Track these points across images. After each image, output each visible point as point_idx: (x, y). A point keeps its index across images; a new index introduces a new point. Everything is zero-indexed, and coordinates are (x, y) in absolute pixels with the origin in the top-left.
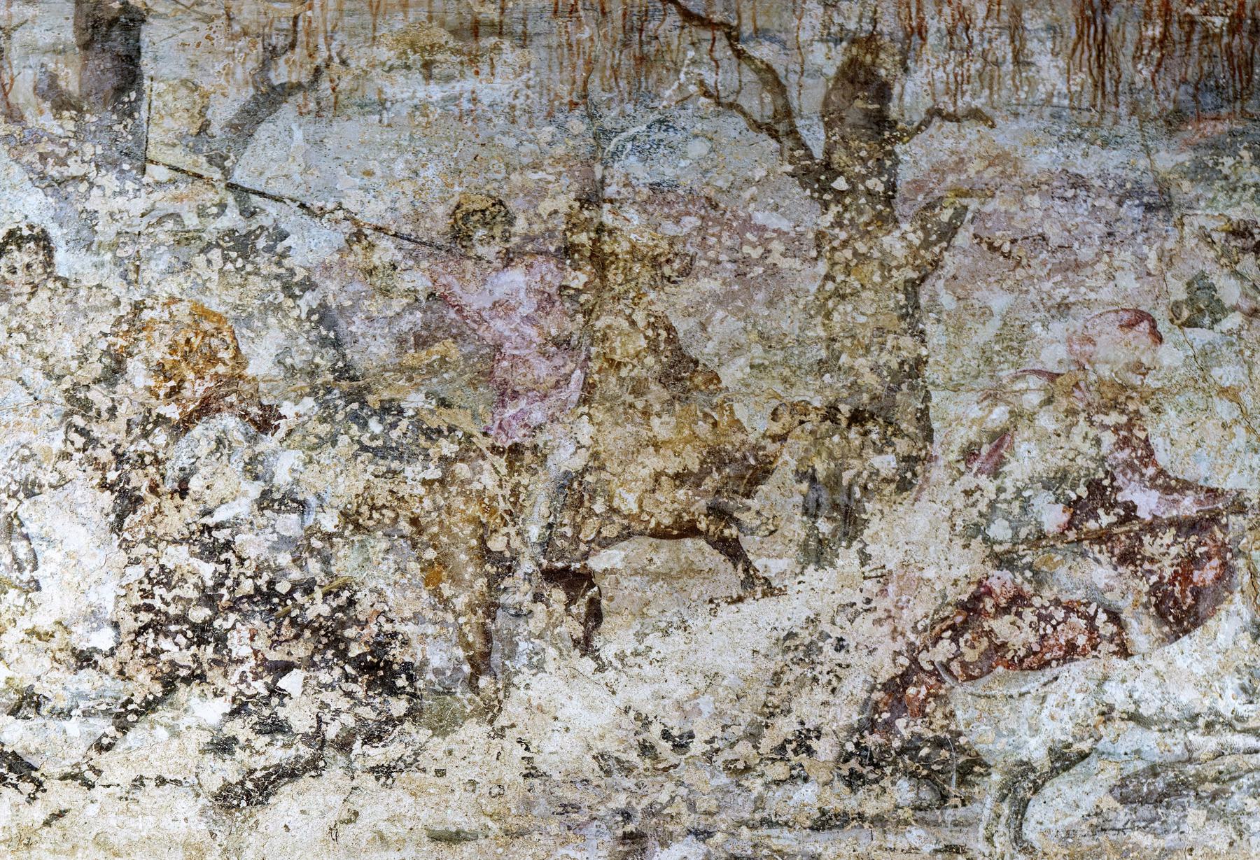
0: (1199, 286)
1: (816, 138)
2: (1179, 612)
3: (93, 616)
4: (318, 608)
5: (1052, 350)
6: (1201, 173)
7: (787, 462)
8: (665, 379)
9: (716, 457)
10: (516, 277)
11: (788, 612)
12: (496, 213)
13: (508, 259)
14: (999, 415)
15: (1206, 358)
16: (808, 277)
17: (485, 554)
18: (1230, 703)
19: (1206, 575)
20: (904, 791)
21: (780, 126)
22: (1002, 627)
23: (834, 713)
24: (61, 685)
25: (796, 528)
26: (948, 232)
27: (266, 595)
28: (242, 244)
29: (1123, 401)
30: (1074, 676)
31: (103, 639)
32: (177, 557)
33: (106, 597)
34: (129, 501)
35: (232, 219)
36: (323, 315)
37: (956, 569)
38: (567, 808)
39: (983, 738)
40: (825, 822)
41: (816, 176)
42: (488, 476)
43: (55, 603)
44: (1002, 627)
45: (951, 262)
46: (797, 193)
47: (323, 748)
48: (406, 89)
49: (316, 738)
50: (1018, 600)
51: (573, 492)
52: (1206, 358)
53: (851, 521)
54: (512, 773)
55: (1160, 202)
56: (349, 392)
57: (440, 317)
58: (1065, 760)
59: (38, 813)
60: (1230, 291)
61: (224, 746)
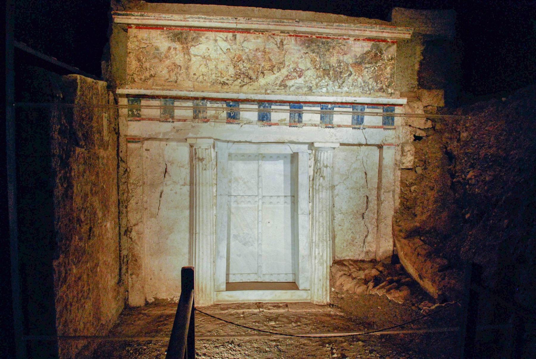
1: (279, 45)
2: (300, 77)
5: (293, 59)
10: (259, 53)
12: (259, 49)
16: (278, 54)
18: (303, 82)
20: (283, 87)
21: (276, 44)
23: (278, 82)
24: (230, 78)
28: (242, 50)
29: (297, 63)
30: (293, 81)
32: (238, 70)
33: (233, 73)
37: (286, 73)
39: (288, 84)
41: (279, 48)
42: (258, 66)
43: (230, 73)
47: (247, 83)
48: (253, 40)
51: (263, 67)
53: (280, 70)
55: (299, 51)
56: (249, 60)
57: (255, 56)
58: (293, 86)
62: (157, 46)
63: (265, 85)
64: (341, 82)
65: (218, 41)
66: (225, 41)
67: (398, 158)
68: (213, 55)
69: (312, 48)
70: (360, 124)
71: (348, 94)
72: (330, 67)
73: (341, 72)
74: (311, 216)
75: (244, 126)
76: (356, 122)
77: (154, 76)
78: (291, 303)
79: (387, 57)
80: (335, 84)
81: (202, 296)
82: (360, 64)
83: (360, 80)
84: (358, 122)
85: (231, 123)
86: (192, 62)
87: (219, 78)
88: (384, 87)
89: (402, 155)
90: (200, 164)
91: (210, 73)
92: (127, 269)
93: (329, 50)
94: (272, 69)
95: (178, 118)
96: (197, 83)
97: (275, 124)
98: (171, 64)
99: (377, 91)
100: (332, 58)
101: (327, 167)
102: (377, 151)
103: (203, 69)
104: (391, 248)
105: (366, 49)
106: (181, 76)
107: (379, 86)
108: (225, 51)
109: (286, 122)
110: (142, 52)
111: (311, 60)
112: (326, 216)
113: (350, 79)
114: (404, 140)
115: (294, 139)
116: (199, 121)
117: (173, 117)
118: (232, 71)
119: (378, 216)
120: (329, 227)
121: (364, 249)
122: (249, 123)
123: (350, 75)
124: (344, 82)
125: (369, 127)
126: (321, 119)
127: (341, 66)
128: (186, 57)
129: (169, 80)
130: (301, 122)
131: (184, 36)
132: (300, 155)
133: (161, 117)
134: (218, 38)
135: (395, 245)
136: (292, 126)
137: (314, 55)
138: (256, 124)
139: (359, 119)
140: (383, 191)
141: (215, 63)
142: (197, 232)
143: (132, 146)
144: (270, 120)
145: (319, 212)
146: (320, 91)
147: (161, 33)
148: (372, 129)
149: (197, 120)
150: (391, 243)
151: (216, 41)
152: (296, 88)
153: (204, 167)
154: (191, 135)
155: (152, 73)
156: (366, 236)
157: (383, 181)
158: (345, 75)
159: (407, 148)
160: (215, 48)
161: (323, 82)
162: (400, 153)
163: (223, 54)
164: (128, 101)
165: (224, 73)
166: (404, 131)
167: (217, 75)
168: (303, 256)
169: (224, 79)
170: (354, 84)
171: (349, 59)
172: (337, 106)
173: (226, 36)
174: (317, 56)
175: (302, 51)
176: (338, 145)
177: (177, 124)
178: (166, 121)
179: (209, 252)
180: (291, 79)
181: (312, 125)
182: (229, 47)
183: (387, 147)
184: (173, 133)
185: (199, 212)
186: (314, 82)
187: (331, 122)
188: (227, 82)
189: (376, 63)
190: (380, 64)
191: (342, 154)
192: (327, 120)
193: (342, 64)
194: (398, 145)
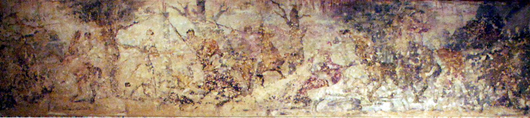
0: (336, 38)
1: (289, 18)
2: (335, 81)
3: (200, 81)
4: (229, 80)
6: (336, 24)
7: (287, 61)
8: (271, 50)
9: (278, 60)
10: (252, 37)
11: (287, 81)
12: (250, 28)
13: (252, 34)
14: (312, 55)
15: (337, 48)
17: (249, 73)
18: (341, 93)
19: (338, 76)
20: (302, 104)
21: (284, 17)
22: (313, 83)
23: (293, 94)
25: (288, 69)
26: (305, 31)
27: (222, 78)
28: (218, 32)
29: (327, 53)
31: (202, 84)
32: (211, 73)
33: (202, 79)
34: (205, 66)
35: (217, 28)
36: (229, 41)
37: (307, 75)
41: (289, 23)
42: (249, 62)
44: (313, 83)
45: (306, 35)
46: (288, 26)
48: (238, 11)
49: (229, 97)
50: (315, 79)
51: (260, 65)
52: (337, 48)
53: (294, 69)
54: (253, 102)
56: (232, 51)
58: (321, 100)
59: (194, 107)
60: (340, 39)
61: (217, 98)
62: (53, 32)
63: (265, 101)
64: (419, 89)
65: (170, 16)
66: (184, 15)
68: (162, 44)
69: (357, 20)
72: (395, 58)
73: (418, 69)
77: (51, 92)
79: (513, 31)
80: (407, 93)
82: (456, 49)
83: (458, 82)
86: (122, 60)
87: (175, 91)
88: (510, 95)
91: (157, 80)
93: (390, 23)
94: (277, 68)
96: (133, 103)
98: (81, 66)
100: (398, 41)
103: (144, 74)
105: (467, 18)
106: (101, 89)
107: (500, 93)
108: (184, 34)
110: (26, 44)
111: (357, 47)
113: (439, 82)
118: (199, 75)
123: (437, 73)
124: (425, 88)
127: (417, 55)
128: (110, 50)
129: (79, 98)
131: (105, 9)
134: (169, 10)
137: (361, 34)
141: (165, 59)
146: (377, 108)
147: (62, 6)
151: (166, 15)
155: (46, 85)
158: (427, 74)
160: (165, 30)
161: (384, 91)
163: (181, 41)
165: (185, 80)
167: (171, 85)
169: (185, 93)
170: (447, 92)
171: (432, 40)
173: (184, 5)
174: (367, 38)
175: (338, 29)
180: (317, 87)
182: (191, 27)
186: (364, 92)
188: (191, 97)
189: (490, 46)
190: (498, 49)
193: (419, 52)
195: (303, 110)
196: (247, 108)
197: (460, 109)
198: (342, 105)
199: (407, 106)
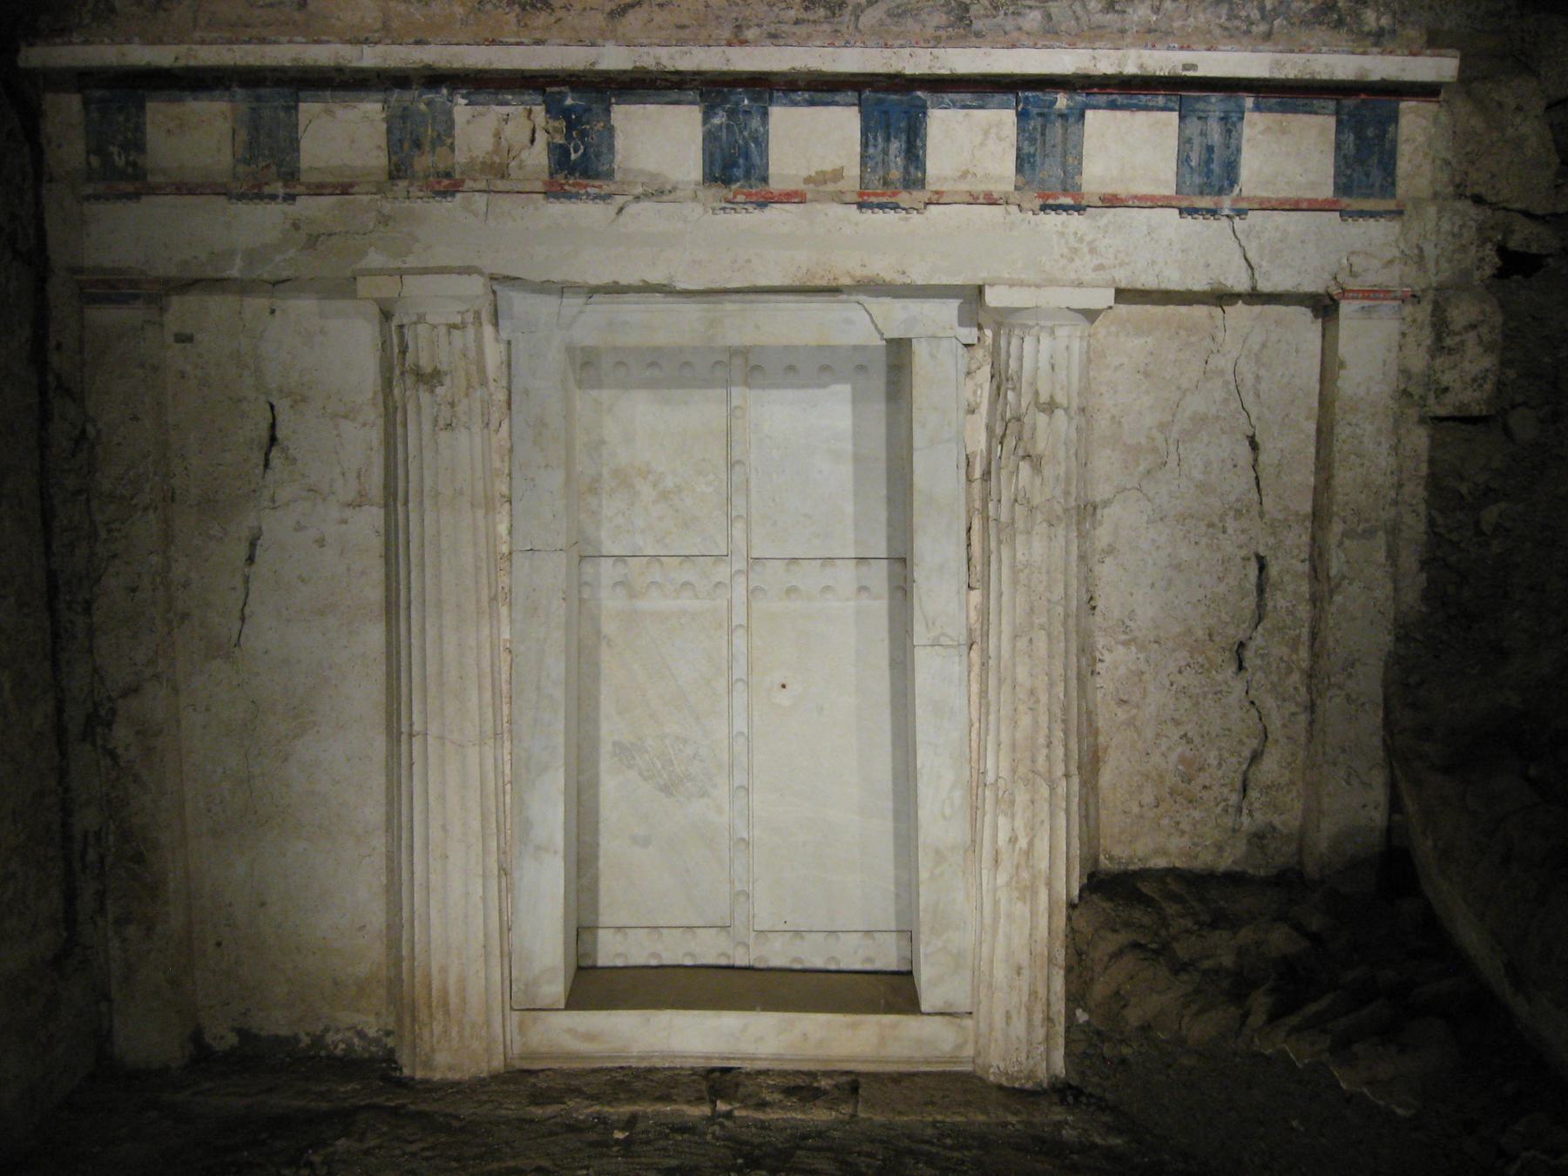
20: (822, 12)
38: (718, 17)
40: (797, 22)
67: (1418, 361)
70: (1221, 191)
71: (1152, 35)
74: (975, 655)
75: (634, 208)
76: (1197, 180)
78: (875, 1077)
81: (446, 1032)
84: (1209, 180)
85: (569, 196)
89: (1438, 348)
90: (425, 397)
92: (101, 896)
95: (315, 178)
97: (789, 197)
99: (1304, 23)
101: (1050, 407)
102: (1304, 327)
104: (1379, 817)
109: (841, 185)
112: (1051, 656)
114: (1446, 273)
115: (882, 267)
116: (414, 191)
117: (291, 175)
119: (1315, 656)
120: (1065, 709)
121: (1246, 820)
122: (659, 192)
125: (1268, 206)
126: (1019, 169)
130: (921, 183)
132: (920, 351)
133: (235, 177)
135: (1395, 804)
136: (871, 206)
138: (695, 198)
139: (1215, 166)
140: (1337, 527)
142: (416, 728)
143: (105, 316)
144: (765, 180)
145: (1015, 637)
146: (1009, 24)
148: (1280, 217)
149: (403, 184)
150: (1379, 794)
152: (890, 14)
153: (445, 413)
154: (375, 259)
156: (1256, 757)
157: (1336, 482)
159: (1461, 313)
162: (1427, 337)
164: (86, 103)
166: (1446, 226)
168: (937, 852)
172: (1103, 99)
176: (1105, 298)
177: (308, 207)
178: (257, 194)
179: (476, 825)
181: (973, 200)
183: (1356, 304)
184: (291, 253)
185: (423, 630)
187: (1069, 183)
191: (1132, 342)
192: (1051, 170)
194: (1416, 298)
195: (826, 27)
196: (685, 21)
197: (1218, 31)
198: (924, 16)
199: (1084, 19)
